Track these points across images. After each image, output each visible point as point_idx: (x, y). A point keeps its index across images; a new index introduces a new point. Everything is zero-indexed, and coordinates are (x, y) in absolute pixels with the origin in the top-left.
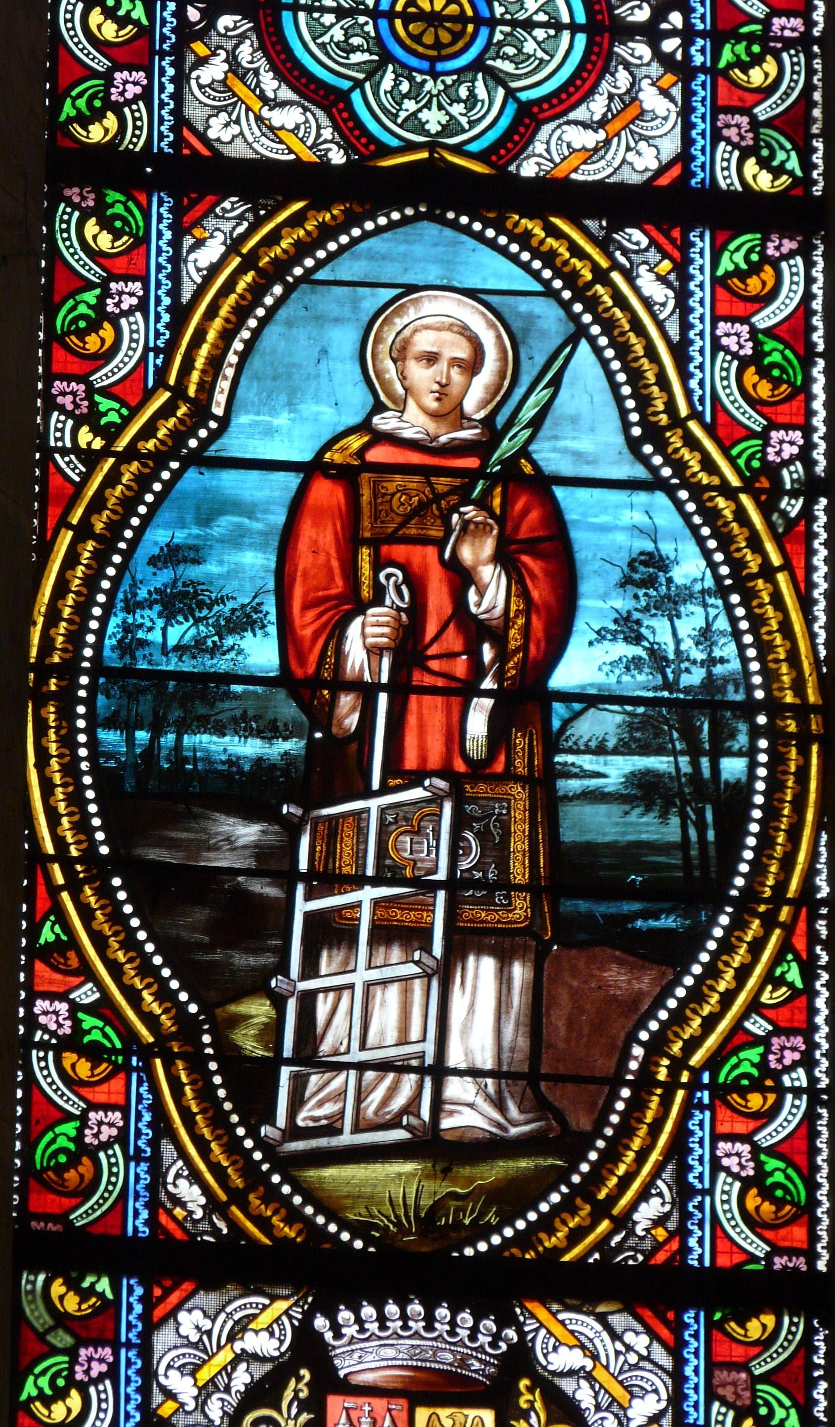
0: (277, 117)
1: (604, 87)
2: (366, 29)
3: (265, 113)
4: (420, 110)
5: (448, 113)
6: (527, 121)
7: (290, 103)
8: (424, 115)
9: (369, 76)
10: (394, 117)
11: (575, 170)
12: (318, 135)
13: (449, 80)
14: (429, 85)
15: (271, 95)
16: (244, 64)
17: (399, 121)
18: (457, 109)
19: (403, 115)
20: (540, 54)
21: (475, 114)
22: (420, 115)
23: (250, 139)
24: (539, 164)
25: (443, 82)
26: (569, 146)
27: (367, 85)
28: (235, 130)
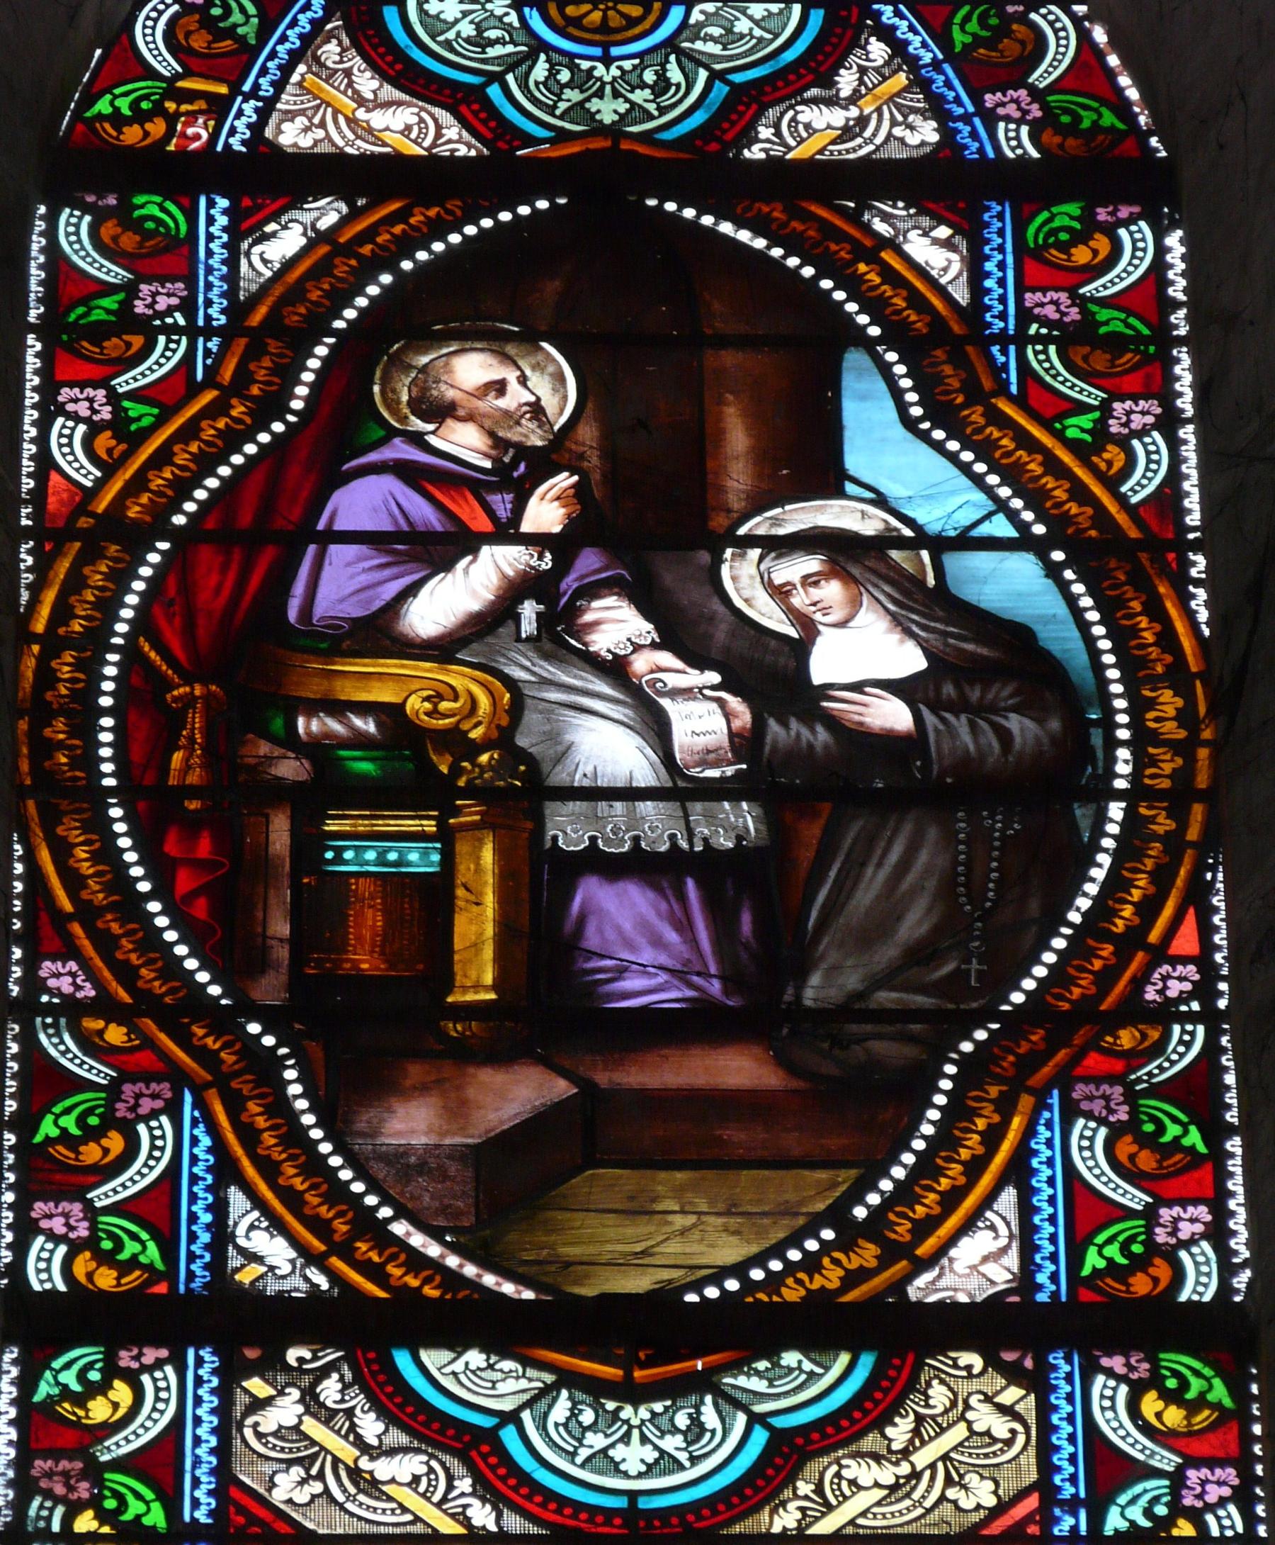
0: (378, 119)
2: (506, 20)
3: (361, 114)
7: (399, 104)
10: (551, 110)
12: (439, 135)
13: (628, 65)
14: (600, 70)
18: (639, 96)
20: (758, 32)
21: (665, 100)
25: (619, 68)
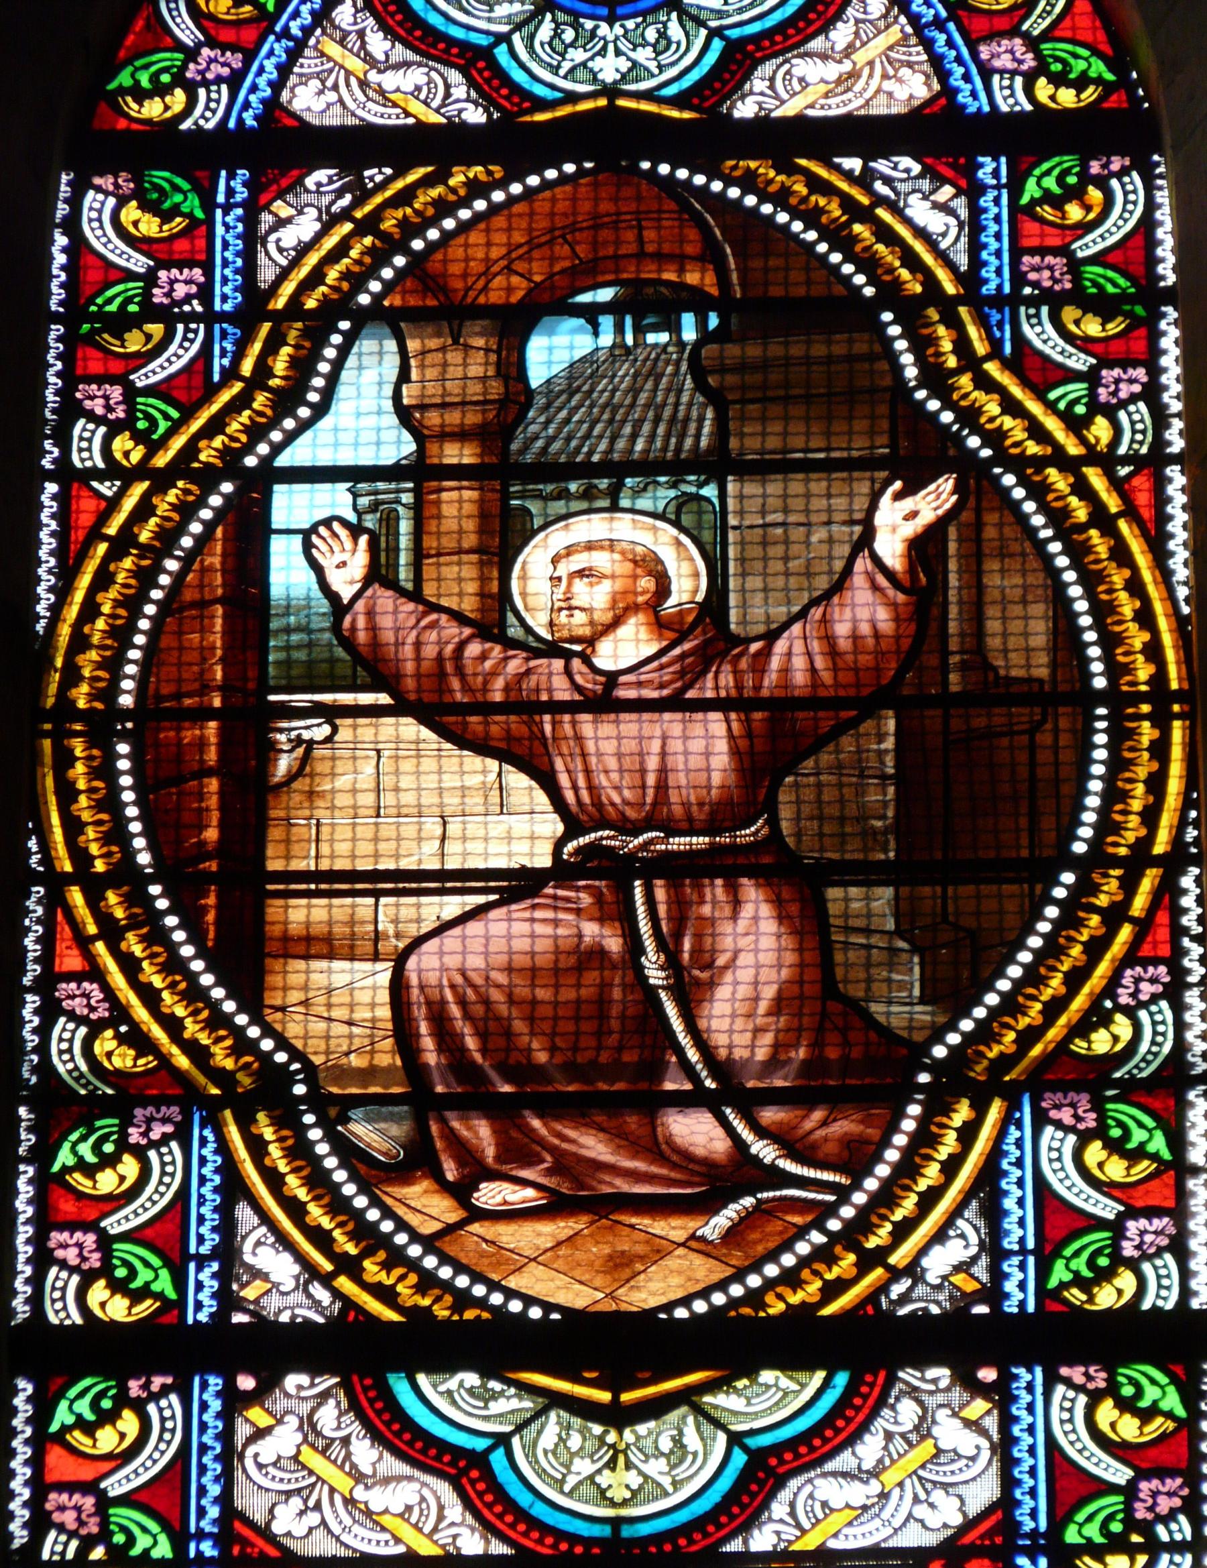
1: (879, 1424)
3: (360, 1493)
4: (599, 1471)
5: (640, 1473)
6: (761, 1475)
7: (399, 1479)
8: (604, 1479)
9: (519, 1428)
11: (835, 1535)
15: (367, 1470)
16: (327, 1432)
17: (567, 1488)
19: (571, 1481)
21: (681, 1472)
22: (598, 1479)
23: (336, 1530)
24: (778, 1533)
26: (824, 1504)
27: (516, 1441)
28: (313, 1519)
